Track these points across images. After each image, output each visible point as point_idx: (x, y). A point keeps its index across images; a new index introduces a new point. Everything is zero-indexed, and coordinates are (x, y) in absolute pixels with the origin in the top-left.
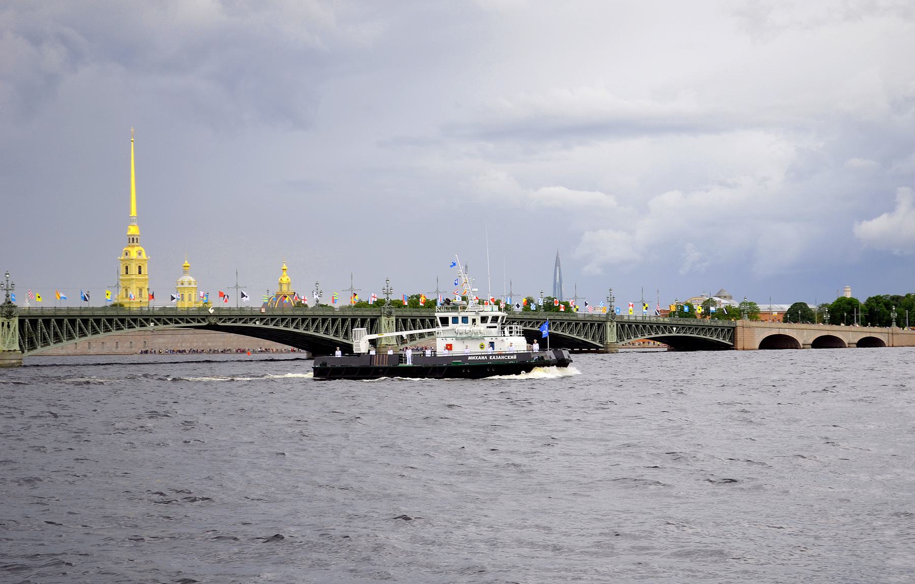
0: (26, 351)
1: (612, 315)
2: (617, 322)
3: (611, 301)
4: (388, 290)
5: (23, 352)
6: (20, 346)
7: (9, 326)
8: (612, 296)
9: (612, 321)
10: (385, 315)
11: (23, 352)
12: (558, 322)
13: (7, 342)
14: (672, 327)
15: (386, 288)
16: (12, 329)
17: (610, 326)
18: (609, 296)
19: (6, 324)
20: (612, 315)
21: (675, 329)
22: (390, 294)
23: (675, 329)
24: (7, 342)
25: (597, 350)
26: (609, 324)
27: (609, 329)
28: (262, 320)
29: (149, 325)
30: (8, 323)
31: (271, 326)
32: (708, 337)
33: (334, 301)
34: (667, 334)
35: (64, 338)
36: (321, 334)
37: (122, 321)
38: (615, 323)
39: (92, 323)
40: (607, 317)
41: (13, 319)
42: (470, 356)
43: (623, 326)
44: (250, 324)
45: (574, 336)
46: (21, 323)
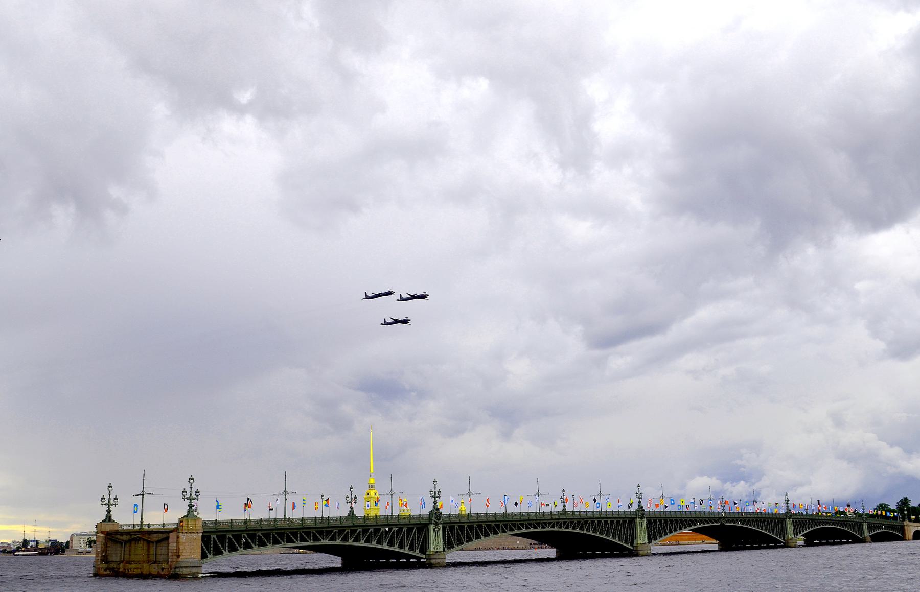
1: (436, 513)
2: (443, 523)
3: (436, 496)
4: (435, 492)
8: (437, 490)
9: (436, 522)
10: (433, 522)
12: (371, 530)
15: (433, 490)
17: (434, 529)
18: (433, 490)
20: (436, 513)
22: (438, 497)
25: (419, 565)
26: (432, 527)
27: (432, 534)
33: (441, 507)
35: (464, 539)
36: (591, 533)
37: (506, 525)
38: (441, 526)
40: (430, 517)
42: (549, 560)
43: (452, 528)
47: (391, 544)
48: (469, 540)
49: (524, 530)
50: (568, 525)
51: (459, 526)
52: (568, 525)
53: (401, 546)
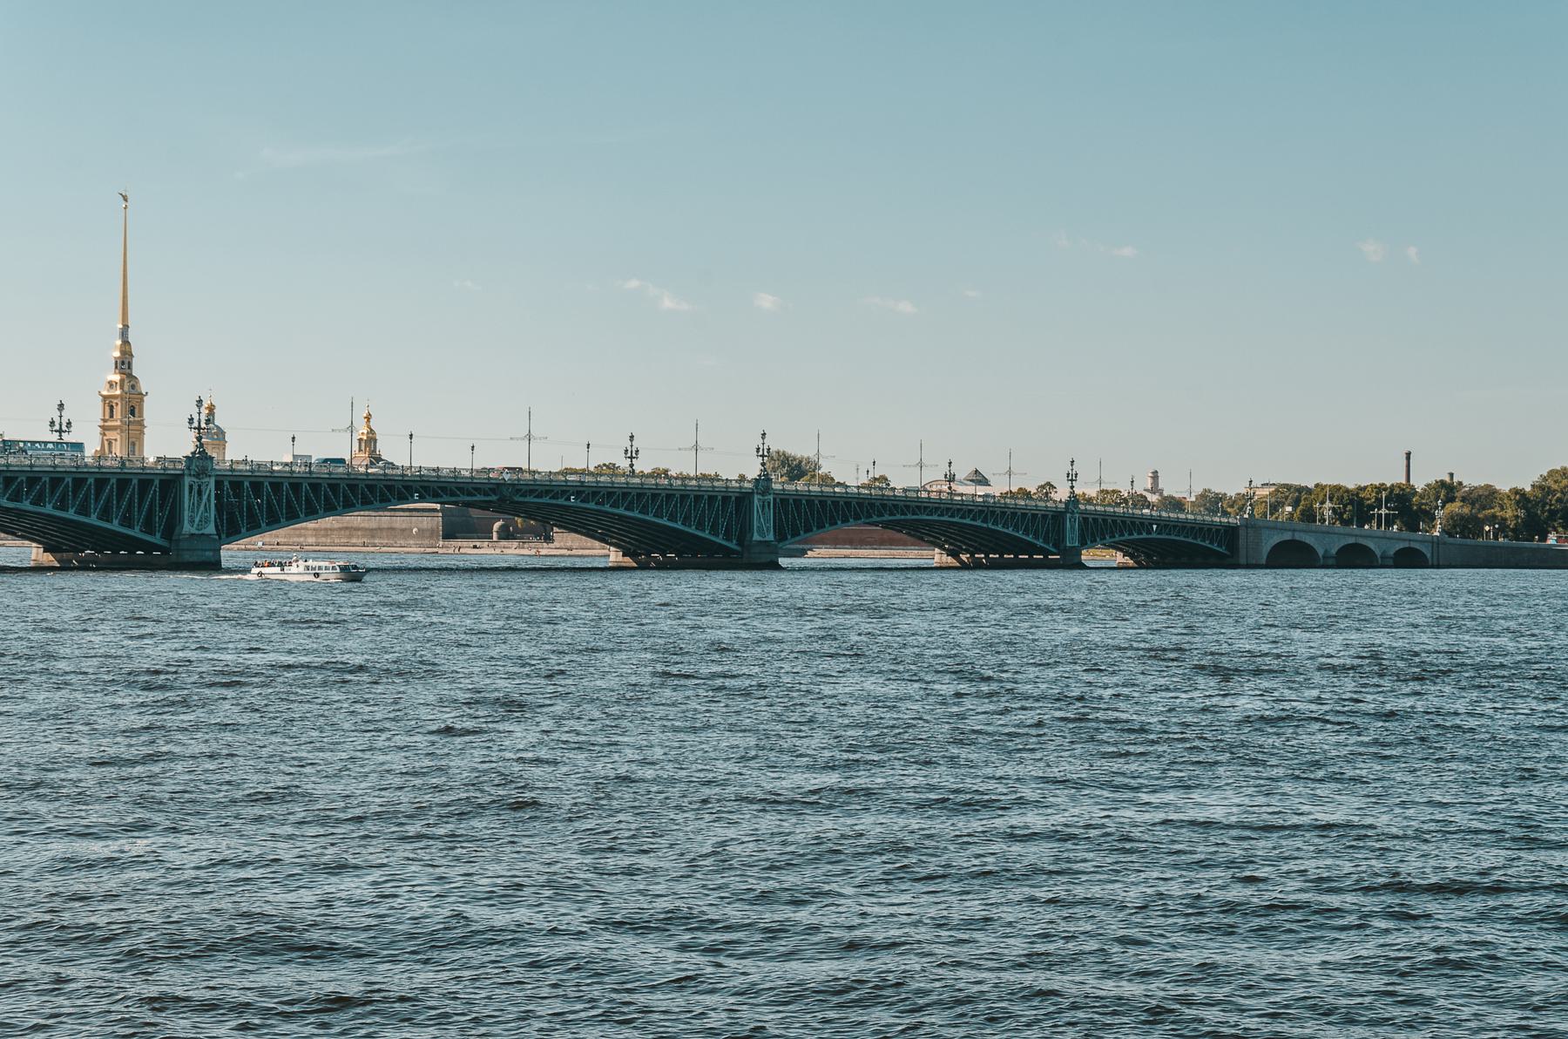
0: (223, 536)
5: (220, 538)
6: (216, 527)
7: (200, 493)
11: (220, 538)
13: (197, 520)
14: (1151, 525)
16: (205, 497)
19: (196, 488)
21: (1155, 527)
23: (1155, 527)
24: (197, 520)
28: (578, 494)
29: (413, 496)
30: (199, 486)
31: (592, 505)
32: (1199, 542)
34: (1144, 535)
39: (325, 490)
41: (207, 480)
44: (561, 501)
45: (1020, 534)
46: (219, 484)
47: (105, 515)
48: (821, 526)
49: (887, 517)
50: (631, 503)
51: (290, 484)
52: (631, 503)
53: (1122, 535)
